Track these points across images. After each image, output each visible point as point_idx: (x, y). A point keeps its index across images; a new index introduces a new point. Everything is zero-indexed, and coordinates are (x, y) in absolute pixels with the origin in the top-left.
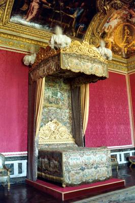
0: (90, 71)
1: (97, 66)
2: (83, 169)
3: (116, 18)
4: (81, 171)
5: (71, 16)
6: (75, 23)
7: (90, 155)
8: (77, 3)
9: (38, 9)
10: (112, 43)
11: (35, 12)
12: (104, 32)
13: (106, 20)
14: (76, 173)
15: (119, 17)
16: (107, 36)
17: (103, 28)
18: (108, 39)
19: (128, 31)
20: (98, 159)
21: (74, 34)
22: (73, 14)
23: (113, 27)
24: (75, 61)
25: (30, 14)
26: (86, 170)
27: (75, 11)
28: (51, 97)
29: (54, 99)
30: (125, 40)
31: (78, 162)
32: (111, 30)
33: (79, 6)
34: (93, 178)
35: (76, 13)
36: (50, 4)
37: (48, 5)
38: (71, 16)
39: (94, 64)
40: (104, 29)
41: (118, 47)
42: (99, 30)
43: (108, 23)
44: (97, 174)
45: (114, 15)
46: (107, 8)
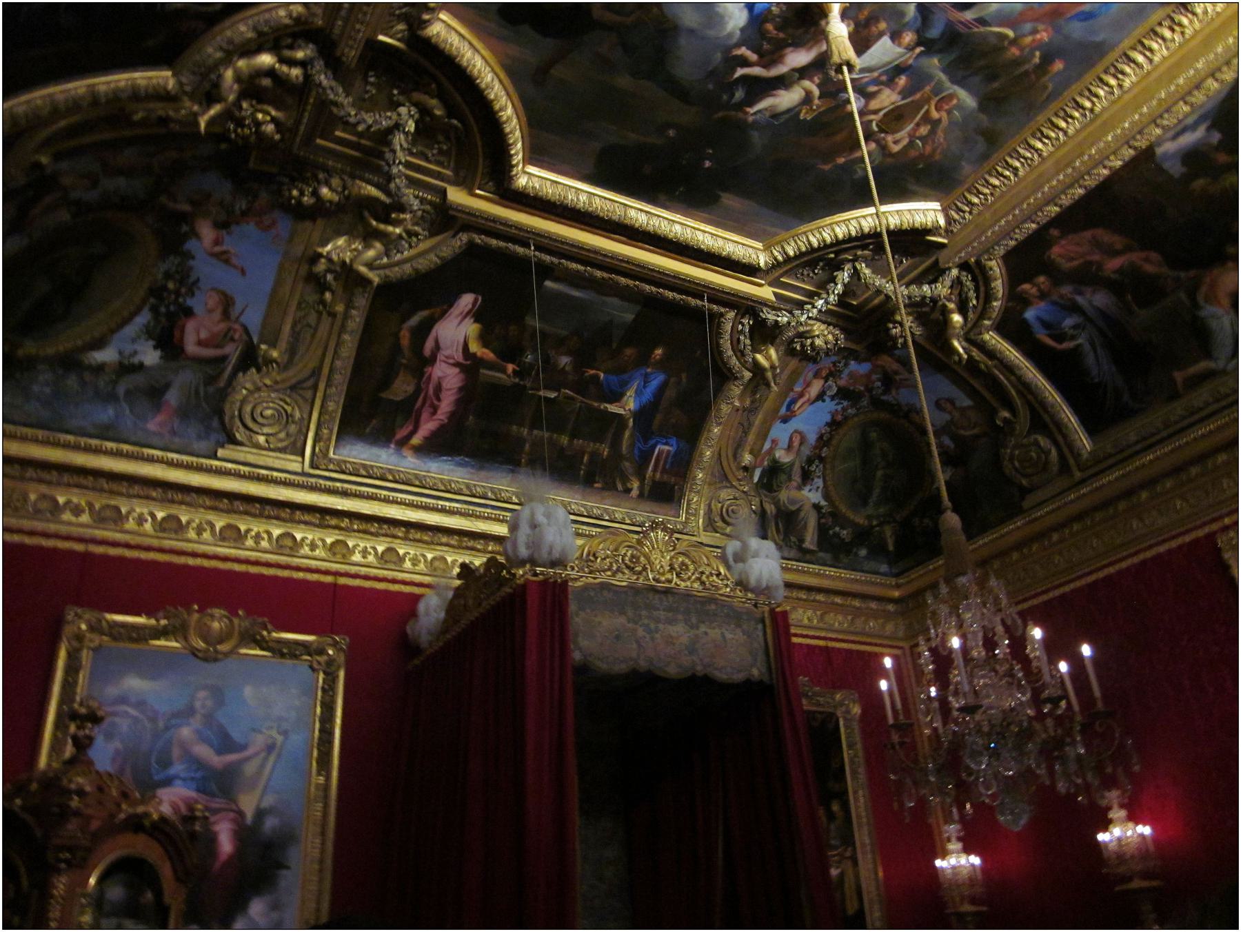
0: (686, 660)
1: (715, 633)
3: (820, 397)
5: (613, 408)
6: (632, 436)
8: (629, 351)
9: (460, 389)
10: (817, 507)
11: (446, 405)
13: (777, 410)
15: (835, 389)
16: (790, 479)
17: (767, 446)
18: (794, 494)
21: (635, 485)
22: (616, 397)
23: (812, 438)
24: (609, 622)
25: (425, 415)
27: (624, 385)
30: (876, 492)
32: (806, 451)
33: (643, 360)
35: (630, 393)
36: (510, 367)
38: (613, 408)
39: (703, 628)
40: (771, 450)
43: (785, 420)
45: (808, 385)
46: (768, 358)
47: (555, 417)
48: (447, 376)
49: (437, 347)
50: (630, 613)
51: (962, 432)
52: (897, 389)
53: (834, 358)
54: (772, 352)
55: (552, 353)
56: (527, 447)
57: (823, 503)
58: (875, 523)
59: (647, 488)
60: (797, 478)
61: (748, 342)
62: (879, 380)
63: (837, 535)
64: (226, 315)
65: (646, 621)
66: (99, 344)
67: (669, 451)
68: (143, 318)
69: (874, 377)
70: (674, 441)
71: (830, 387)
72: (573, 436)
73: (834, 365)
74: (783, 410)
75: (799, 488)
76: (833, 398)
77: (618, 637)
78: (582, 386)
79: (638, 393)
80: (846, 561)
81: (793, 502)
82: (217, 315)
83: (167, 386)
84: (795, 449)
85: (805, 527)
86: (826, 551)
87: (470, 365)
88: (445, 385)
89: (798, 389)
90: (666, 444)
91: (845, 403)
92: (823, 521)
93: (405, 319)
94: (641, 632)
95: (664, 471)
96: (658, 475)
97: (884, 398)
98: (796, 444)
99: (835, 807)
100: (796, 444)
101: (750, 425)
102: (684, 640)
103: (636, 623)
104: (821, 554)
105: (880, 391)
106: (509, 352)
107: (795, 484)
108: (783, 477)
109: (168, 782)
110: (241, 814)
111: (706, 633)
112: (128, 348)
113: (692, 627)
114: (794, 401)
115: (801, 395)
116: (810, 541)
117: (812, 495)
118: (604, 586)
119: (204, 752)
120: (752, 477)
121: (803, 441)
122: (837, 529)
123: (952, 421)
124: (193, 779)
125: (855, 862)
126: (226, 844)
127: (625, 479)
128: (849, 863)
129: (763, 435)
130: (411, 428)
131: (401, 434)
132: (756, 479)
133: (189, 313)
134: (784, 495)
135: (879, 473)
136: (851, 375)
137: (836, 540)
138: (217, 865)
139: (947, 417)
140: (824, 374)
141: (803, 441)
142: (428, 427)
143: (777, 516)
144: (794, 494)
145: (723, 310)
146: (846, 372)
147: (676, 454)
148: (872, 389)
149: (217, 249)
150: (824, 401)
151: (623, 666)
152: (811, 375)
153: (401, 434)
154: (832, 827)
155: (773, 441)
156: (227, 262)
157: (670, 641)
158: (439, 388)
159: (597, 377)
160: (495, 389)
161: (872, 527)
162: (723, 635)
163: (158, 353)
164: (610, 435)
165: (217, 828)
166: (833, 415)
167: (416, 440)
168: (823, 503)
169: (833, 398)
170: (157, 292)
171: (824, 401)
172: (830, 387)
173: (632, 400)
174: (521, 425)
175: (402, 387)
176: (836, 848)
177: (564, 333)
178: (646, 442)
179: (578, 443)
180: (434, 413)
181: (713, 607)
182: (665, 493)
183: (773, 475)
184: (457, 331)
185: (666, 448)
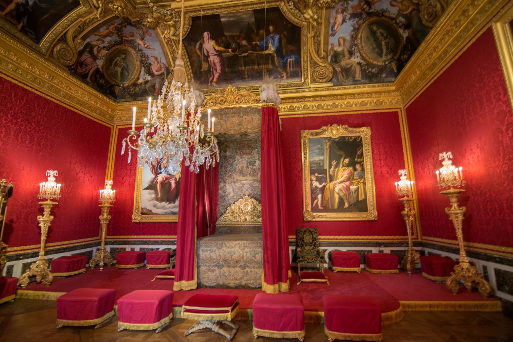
0: (237, 128)
3: (344, 21)
4: (216, 268)
6: (277, 59)
7: (232, 247)
9: (220, 62)
10: (359, 64)
11: (219, 67)
12: (335, 52)
13: (328, 32)
14: (209, 270)
15: (349, 16)
16: (344, 56)
19: (381, 30)
20: (249, 254)
21: (285, 74)
22: (267, 48)
23: (348, 38)
25: (214, 72)
26: (225, 269)
27: (267, 43)
28: (245, 168)
29: (250, 169)
30: (385, 51)
31: (213, 255)
32: (348, 45)
33: (268, 33)
34: (237, 282)
35: (270, 45)
36: (230, 50)
37: (228, 52)
38: (267, 52)
41: (373, 66)
42: (323, 53)
43: (333, 35)
44: (245, 278)
45: (336, 18)
47: (248, 61)
48: (214, 59)
49: (208, 52)
50: (219, 117)
51: (405, 13)
52: (373, 4)
53: (341, 3)
54: (310, 12)
55: (239, 41)
56: (246, 72)
57: (362, 61)
58: (387, 63)
59: (289, 75)
60: (347, 55)
61: (297, 11)
62: (364, 4)
63: (371, 72)
64: (158, 62)
66: (138, 79)
67: (293, 61)
68: (143, 69)
69: (362, 4)
70: (293, 56)
71: (346, 16)
72: (258, 65)
73: (342, 5)
74: (330, 32)
75: (349, 58)
76: (350, 19)
78: (254, 48)
79: (273, 44)
80: (375, 81)
81: (348, 64)
82: (156, 63)
83: (155, 84)
84: (342, 45)
85: (355, 72)
86: (366, 79)
87: (219, 54)
88: (216, 62)
89: (332, 21)
90: (291, 58)
91: (356, 20)
92: (363, 68)
93: (195, 47)
94: (222, 122)
95: (293, 67)
96: (292, 69)
97: (370, 11)
98: (342, 42)
99: (358, 166)
100: (342, 42)
101: (320, 42)
102: (237, 122)
104: (362, 81)
105: (368, 9)
106: (227, 46)
107: (346, 58)
108: (341, 56)
109: (161, 173)
110: (176, 178)
112: (144, 77)
114: (333, 27)
115: (335, 23)
116: (358, 75)
117: (356, 60)
120: (328, 60)
121: (344, 40)
122: (370, 70)
123: (399, 9)
125: (364, 184)
126: (173, 185)
127: (281, 74)
128: (362, 184)
129: (326, 43)
131: (210, 79)
132: (329, 60)
133: (150, 64)
134: (343, 63)
135: (383, 43)
136: (352, 7)
137: (370, 74)
139: (397, 8)
140: (340, 10)
141: (344, 40)
142: (216, 75)
143: (342, 72)
144: (348, 61)
145: (278, 3)
146: (349, 7)
147: (295, 60)
148: (364, 9)
149: (146, 46)
150: (346, 22)
152: (334, 14)
153: (210, 79)
154: (356, 173)
155: (332, 45)
156: (149, 48)
157: (232, 123)
158: (214, 64)
159: (256, 44)
160: (229, 58)
161: (386, 65)
162: (252, 118)
163: (150, 77)
164: (270, 61)
166: (353, 26)
167: (215, 80)
168: (362, 61)
169: (350, 19)
170: (142, 62)
171: (346, 22)
172: (346, 16)
173: (272, 47)
174: (241, 66)
176: (357, 179)
177: (238, 33)
178: (283, 59)
179: (261, 67)
180: (217, 71)
181: (249, 109)
182: (296, 74)
183: (336, 57)
184: (209, 45)
185: (291, 59)
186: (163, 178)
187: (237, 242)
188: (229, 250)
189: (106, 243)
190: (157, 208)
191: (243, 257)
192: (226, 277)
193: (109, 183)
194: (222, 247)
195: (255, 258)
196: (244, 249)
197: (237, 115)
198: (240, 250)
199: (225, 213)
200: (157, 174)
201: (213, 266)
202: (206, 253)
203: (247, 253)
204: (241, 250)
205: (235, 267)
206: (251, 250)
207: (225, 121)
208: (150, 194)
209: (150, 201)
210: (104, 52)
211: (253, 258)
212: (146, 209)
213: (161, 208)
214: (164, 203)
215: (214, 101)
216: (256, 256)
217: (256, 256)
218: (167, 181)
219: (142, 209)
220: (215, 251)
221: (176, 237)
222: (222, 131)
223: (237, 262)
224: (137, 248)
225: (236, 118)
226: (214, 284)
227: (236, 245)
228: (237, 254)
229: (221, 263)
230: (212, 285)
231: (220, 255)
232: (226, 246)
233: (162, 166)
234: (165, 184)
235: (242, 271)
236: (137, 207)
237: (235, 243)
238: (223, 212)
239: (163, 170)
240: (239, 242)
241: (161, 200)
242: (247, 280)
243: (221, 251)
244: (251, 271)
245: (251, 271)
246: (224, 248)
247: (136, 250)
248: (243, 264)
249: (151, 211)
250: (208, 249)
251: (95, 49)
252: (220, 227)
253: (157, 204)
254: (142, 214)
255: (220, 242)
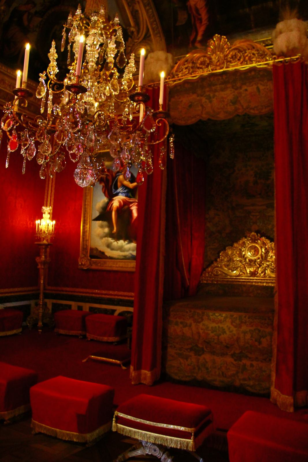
0: (230, 108)
2: (199, 352)
4: (192, 354)
7: (220, 322)
11: (204, 16)
20: (248, 336)
25: (198, 25)
65: (208, 93)
77: (190, 106)
88: (198, 7)
94: (204, 100)
102: (231, 97)
103: (202, 96)
109: (117, 194)
111: (246, 90)
113: (236, 89)
118: (187, 82)
119: (126, 183)
124: (124, 192)
130: (195, 34)
131: (192, 38)
138: (133, 220)
151: (193, 120)
153: (192, 38)
158: (197, 10)
162: (258, 88)
165: (132, 208)
167: (199, 38)
175: (182, 17)
180: (201, 22)
181: (253, 73)
186: (120, 203)
187: (228, 314)
188: (214, 325)
189: (46, 296)
190: (112, 249)
191: (238, 339)
192: (207, 369)
193: (47, 210)
194: (202, 320)
195: (260, 343)
196: (240, 327)
197: (229, 85)
198: (232, 328)
199: (216, 261)
200: (111, 196)
201: (187, 349)
202: (176, 327)
203: (245, 333)
204: (235, 327)
205: (223, 354)
206: (252, 328)
207: (209, 98)
208: (102, 227)
209: (102, 238)
210: (37, 20)
211: (257, 343)
212: (97, 249)
213: (117, 250)
214: (121, 242)
215: (190, 65)
216: (262, 339)
217: (262, 339)
218: (126, 207)
219: (92, 249)
220: (190, 326)
221: (133, 294)
222: (204, 116)
223: (227, 347)
224: (86, 307)
225: (228, 92)
226: (188, 379)
227: (226, 318)
228: (228, 332)
229: (200, 345)
230: (184, 379)
231: (199, 333)
232: (209, 319)
233: (119, 184)
234: (124, 210)
235: (234, 363)
236: (85, 247)
237: (224, 315)
238: (213, 259)
239: (120, 190)
240: (232, 313)
241: (117, 237)
242: (244, 379)
243: (201, 325)
244: (252, 365)
245: (252, 365)
246: (206, 322)
247: (84, 310)
248: (237, 352)
249: (103, 253)
250: (179, 321)
251: (25, 17)
252: (207, 285)
253: (111, 243)
254: (92, 257)
255: (200, 312)
